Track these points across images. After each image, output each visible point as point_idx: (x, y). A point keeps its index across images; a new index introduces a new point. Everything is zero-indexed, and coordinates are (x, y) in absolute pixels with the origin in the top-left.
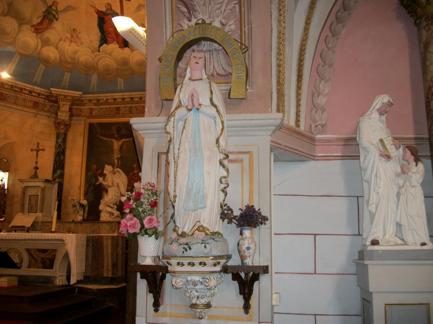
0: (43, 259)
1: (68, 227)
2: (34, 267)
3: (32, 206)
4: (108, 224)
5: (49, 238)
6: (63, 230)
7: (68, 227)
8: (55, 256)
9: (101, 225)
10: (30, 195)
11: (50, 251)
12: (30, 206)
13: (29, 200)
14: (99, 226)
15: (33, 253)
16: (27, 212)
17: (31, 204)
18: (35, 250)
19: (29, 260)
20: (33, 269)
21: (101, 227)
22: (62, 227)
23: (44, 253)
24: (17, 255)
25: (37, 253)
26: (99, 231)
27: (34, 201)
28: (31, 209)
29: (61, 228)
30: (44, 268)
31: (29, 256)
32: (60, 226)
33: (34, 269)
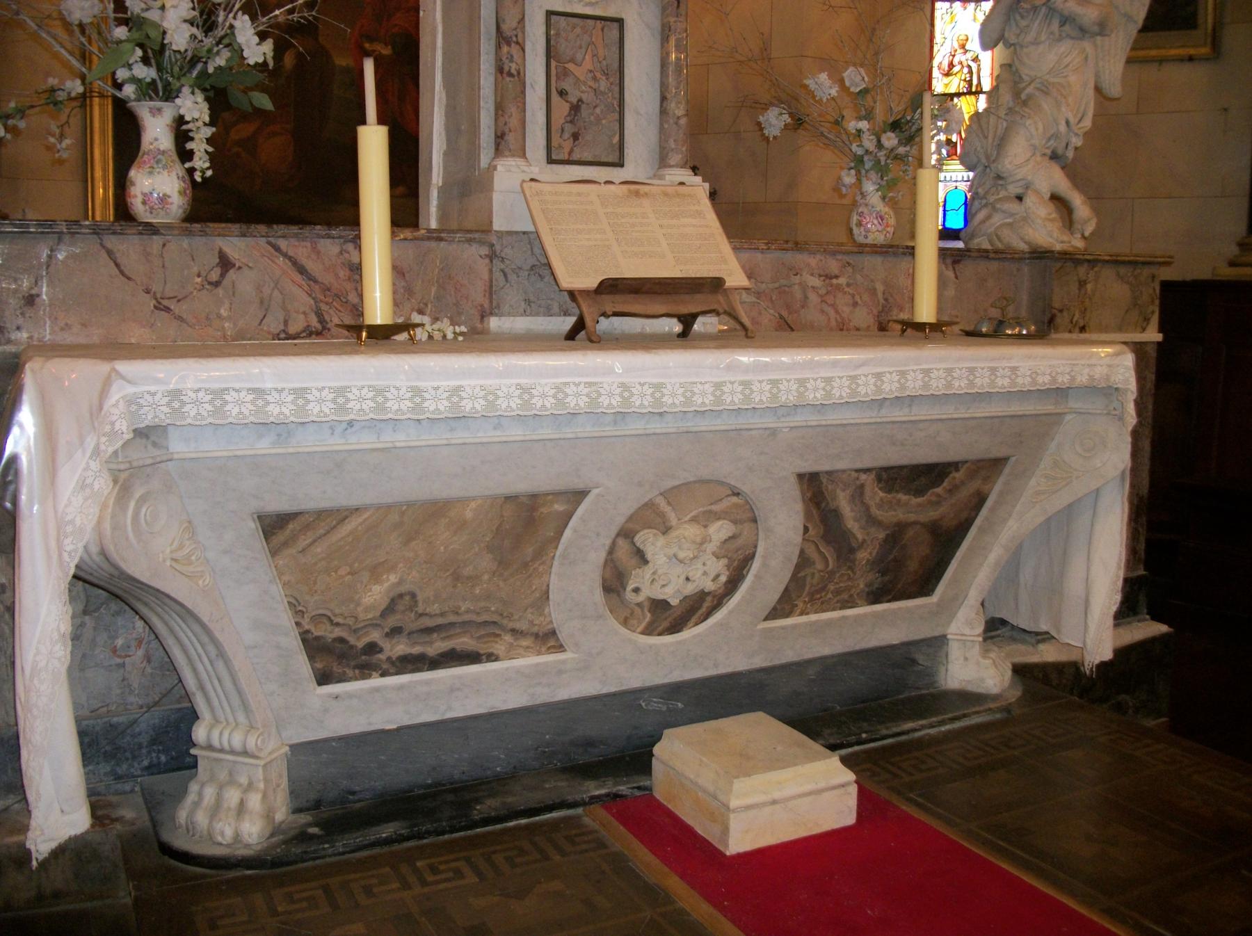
0: (896, 535)
1: (880, 288)
2: (818, 600)
3: (576, 108)
4: (1123, 270)
5: (1040, 379)
6: (855, 304)
7: (880, 288)
8: (980, 500)
9: (1092, 274)
10: (550, 14)
11: (958, 475)
12: (561, 109)
13: (549, 53)
14: (1082, 284)
15: (843, 502)
16: (542, 153)
17: (566, 85)
18: (863, 477)
19: (802, 552)
20: (804, 619)
21: (1089, 287)
22: (842, 281)
23: (919, 492)
24: (720, 531)
25: (875, 494)
26: (1084, 312)
27: (588, 64)
28: (575, 137)
29: (838, 287)
30: (876, 596)
31: (806, 529)
32: (829, 277)
33: (813, 617)
